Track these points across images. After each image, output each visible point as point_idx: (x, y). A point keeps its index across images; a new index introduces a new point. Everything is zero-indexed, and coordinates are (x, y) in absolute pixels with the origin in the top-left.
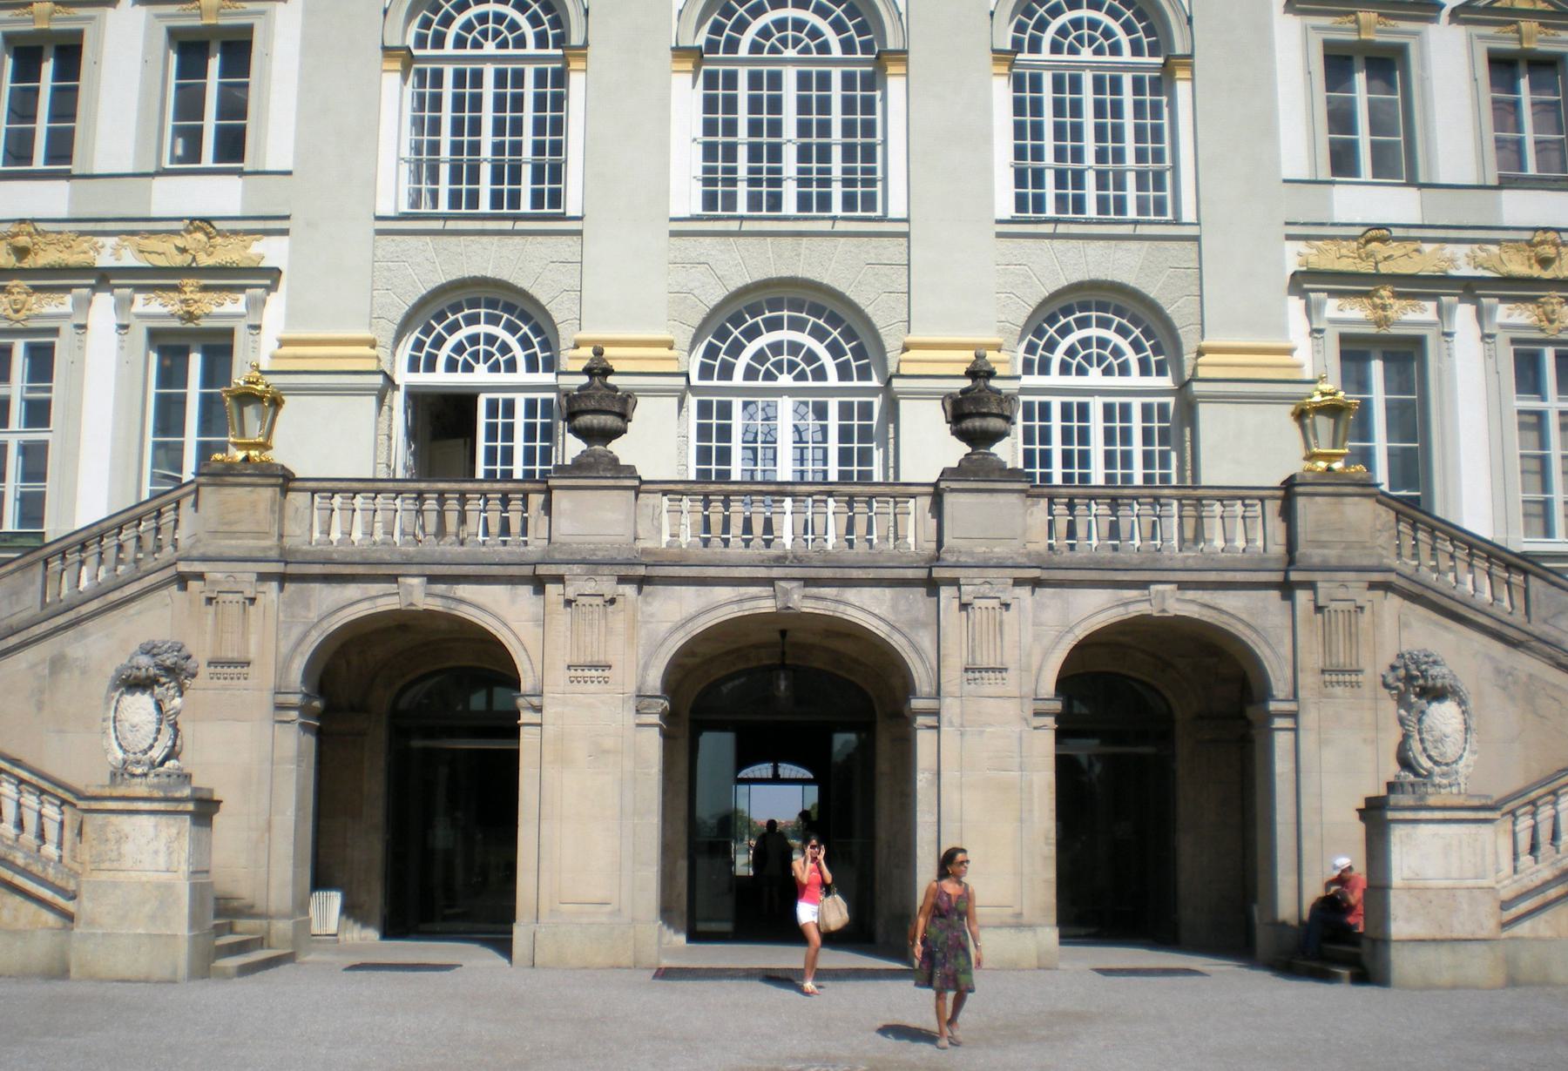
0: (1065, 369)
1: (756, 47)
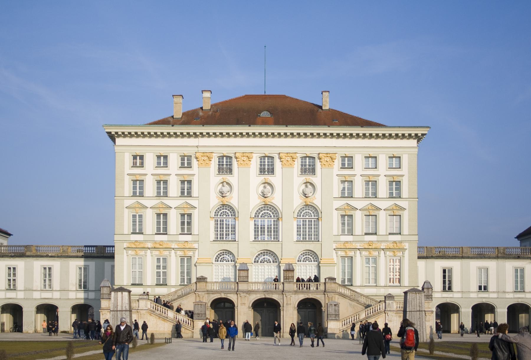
1: (261, 216)
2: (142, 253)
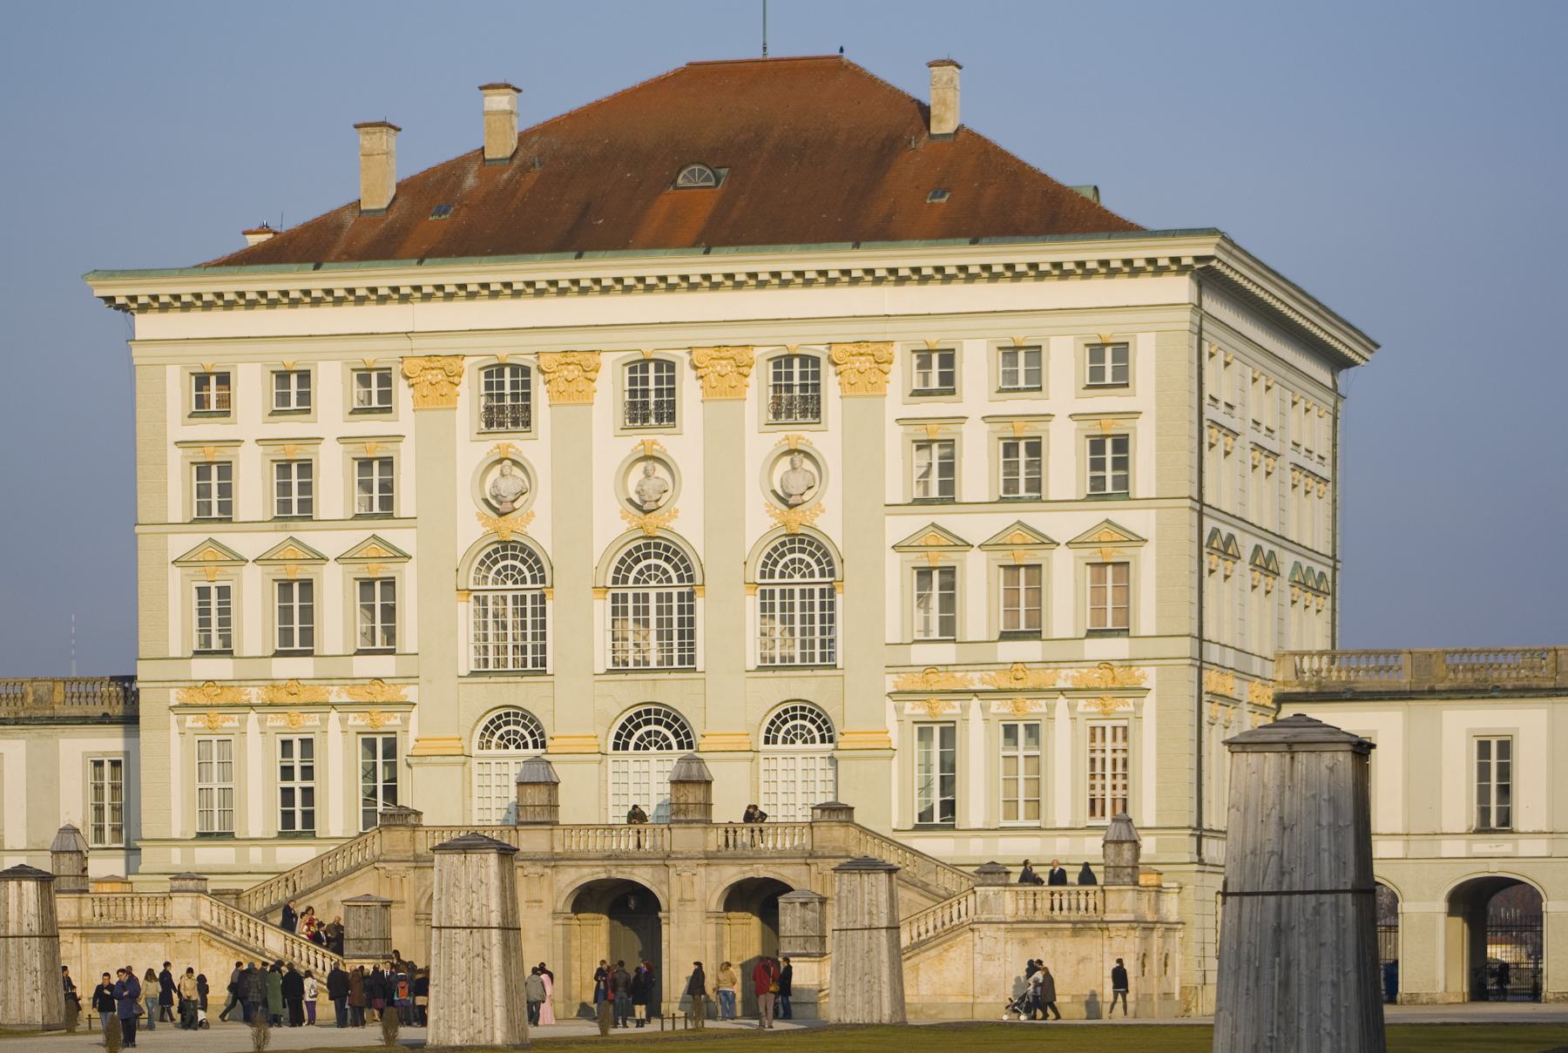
0: (785, 741)
1: (636, 580)
2: (231, 722)
